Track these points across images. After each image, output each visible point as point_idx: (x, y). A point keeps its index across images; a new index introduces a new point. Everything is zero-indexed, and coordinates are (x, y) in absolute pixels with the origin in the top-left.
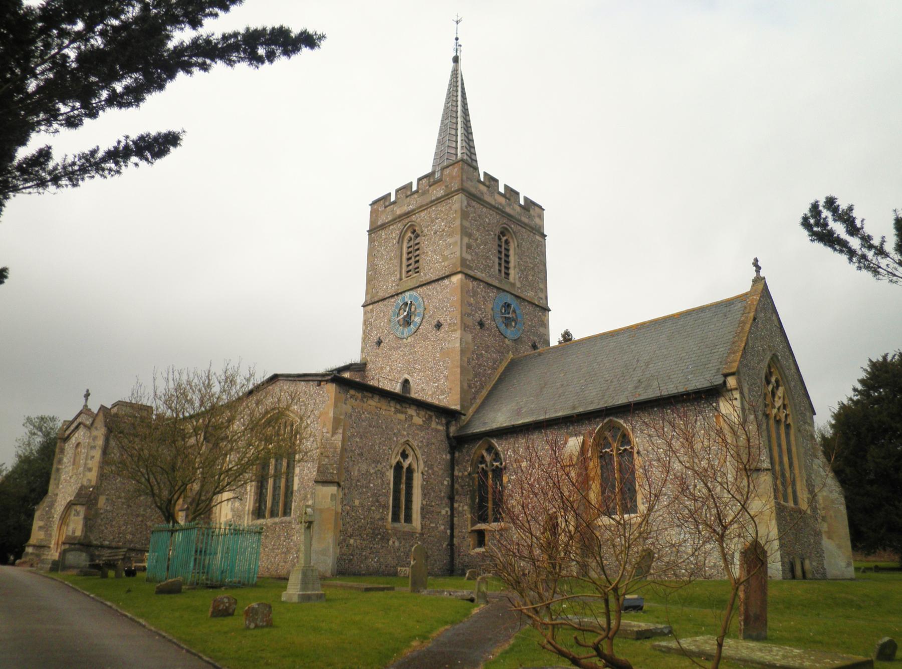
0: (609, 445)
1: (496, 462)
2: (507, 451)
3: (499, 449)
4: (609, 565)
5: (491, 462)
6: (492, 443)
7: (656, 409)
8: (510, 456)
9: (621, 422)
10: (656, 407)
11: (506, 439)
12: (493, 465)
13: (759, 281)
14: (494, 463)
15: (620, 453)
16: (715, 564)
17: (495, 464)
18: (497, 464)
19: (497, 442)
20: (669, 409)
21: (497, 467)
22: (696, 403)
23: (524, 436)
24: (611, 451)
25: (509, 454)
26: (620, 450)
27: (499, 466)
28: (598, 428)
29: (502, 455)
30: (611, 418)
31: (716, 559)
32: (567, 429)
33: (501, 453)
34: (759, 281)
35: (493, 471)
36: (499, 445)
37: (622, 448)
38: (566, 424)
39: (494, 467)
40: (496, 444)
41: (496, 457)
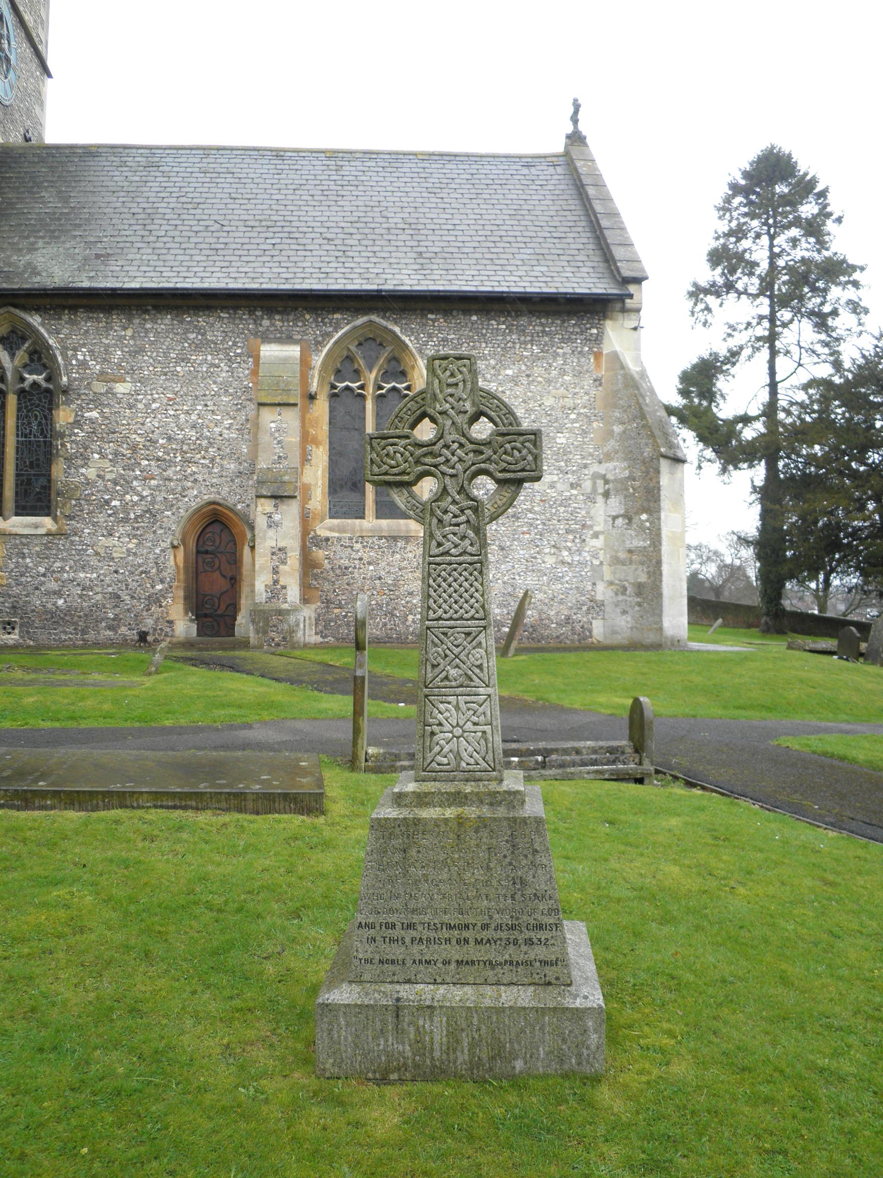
0: (357, 374)
1: (30, 374)
2: (75, 350)
3: (51, 342)
4: (345, 616)
5: (16, 370)
6: (29, 325)
7: (474, 318)
8: (83, 364)
9: (397, 329)
10: (476, 314)
11: (71, 322)
12: (22, 380)
13: (576, 139)
14: (27, 376)
15: (381, 396)
16: (568, 618)
17: (30, 378)
18: (39, 378)
19: (43, 324)
20: (504, 323)
21: (35, 384)
22: (559, 322)
23: (130, 321)
24: (362, 387)
25: (80, 357)
26: (381, 388)
27: (44, 384)
28: (337, 336)
29: (60, 359)
30: (374, 318)
31: (571, 608)
32: (255, 323)
33: (58, 353)
34: (576, 139)
35: (21, 393)
36: (49, 333)
37: (388, 386)
38: (251, 312)
39: (26, 385)
40: (42, 330)
41: (32, 360)
